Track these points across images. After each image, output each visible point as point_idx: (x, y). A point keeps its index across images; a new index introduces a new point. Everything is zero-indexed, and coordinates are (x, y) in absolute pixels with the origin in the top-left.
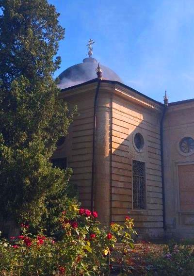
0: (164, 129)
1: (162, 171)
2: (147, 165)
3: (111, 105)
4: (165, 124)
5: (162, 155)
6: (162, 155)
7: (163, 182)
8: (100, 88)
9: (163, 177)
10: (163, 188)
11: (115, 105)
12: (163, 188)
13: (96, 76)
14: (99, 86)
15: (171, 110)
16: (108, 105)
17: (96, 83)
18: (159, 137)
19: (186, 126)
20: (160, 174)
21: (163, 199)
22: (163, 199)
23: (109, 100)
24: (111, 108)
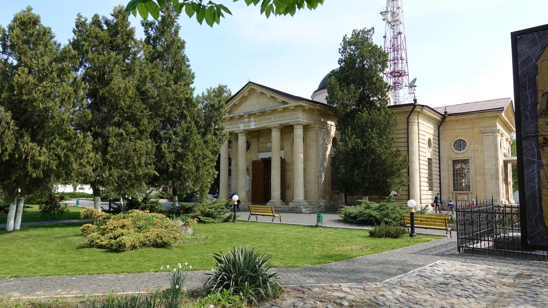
0: (441, 133)
1: (439, 164)
2: (433, 161)
3: (418, 120)
4: (441, 128)
5: (439, 152)
6: (439, 152)
7: (440, 172)
8: (415, 109)
9: (439, 168)
10: (440, 175)
11: (420, 121)
12: (440, 175)
13: (413, 102)
14: (414, 108)
15: (448, 119)
16: (417, 121)
17: (413, 107)
18: (437, 138)
19: (459, 131)
20: (438, 166)
21: (440, 183)
22: (440, 183)
23: (416, 117)
24: (418, 123)
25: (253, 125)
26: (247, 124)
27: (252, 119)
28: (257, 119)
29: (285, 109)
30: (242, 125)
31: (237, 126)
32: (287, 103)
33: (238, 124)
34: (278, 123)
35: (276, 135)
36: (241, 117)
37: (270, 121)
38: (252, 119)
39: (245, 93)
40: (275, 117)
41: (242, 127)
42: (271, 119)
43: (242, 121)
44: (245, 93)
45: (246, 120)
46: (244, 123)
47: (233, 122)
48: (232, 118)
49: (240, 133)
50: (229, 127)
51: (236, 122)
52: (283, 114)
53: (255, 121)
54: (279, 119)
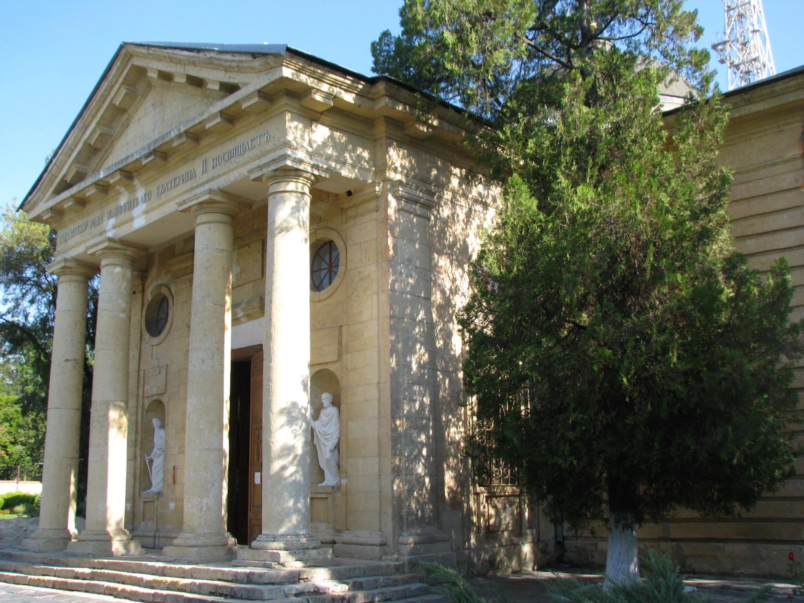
26: (123, 216)
28: (154, 188)
29: (231, 117)
30: (112, 222)
31: (97, 230)
34: (214, 185)
37: (188, 185)
39: (118, 95)
40: (205, 162)
41: (111, 228)
43: (112, 206)
44: (118, 95)
45: (123, 200)
46: (119, 211)
52: (230, 146)
54: (217, 171)
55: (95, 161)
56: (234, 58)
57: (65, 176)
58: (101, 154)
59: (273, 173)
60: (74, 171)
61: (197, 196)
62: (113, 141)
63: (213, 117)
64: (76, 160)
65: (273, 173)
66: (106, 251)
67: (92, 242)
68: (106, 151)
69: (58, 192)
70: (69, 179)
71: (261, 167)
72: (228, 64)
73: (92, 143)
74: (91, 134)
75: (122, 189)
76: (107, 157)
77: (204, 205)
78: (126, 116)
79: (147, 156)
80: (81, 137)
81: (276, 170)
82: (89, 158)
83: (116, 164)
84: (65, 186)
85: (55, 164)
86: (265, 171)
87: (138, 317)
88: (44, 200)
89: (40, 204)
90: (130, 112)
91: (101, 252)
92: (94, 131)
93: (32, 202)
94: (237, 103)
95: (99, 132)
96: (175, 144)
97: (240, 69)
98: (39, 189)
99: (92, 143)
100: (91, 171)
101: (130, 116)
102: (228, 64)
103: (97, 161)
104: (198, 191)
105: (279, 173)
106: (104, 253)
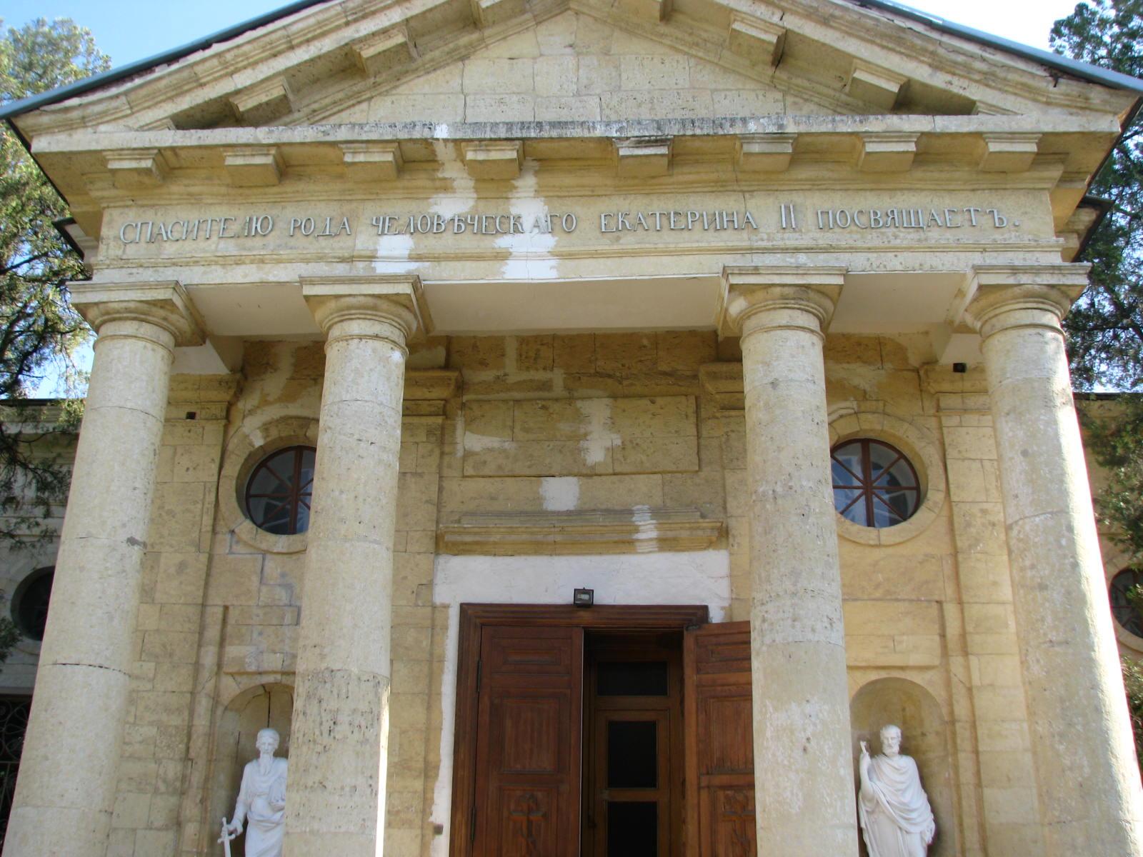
25: (532, 257)
27: (528, 205)
32: (966, 108)
33: (344, 228)
35: (788, 374)
36: (413, 161)
37: (730, 238)
38: (528, 205)
41: (394, 255)
42: (748, 225)
46: (427, 226)
47: (290, 213)
48: (287, 168)
49: (373, 307)
50: (229, 247)
51: (322, 211)
53: (560, 224)
55: (336, 92)
56: (986, 55)
57: (238, 92)
58: (360, 86)
59: (1045, 290)
60: (276, 92)
61: (799, 270)
62: (407, 72)
63: (901, 136)
64: (291, 74)
65: (1045, 290)
66: (384, 305)
67: (322, 269)
68: (375, 85)
69: (183, 122)
70: (244, 105)
71: (1014, 270)
72: (960, 59)
73: (367, 53)
74: (374, 34)
75: (463, 181)
76: (370, 99)
77: (812, 294)
78: (475, 36)
79: (641, 142)
80: (338, 28)
81: (1052, 286)
82: (316, 81)
83: (510, 126)
84: (222, 114)
85: (219, 55)
86: (1025, 279)
87: (207, 471)
88: (131, 122)
89: (103, 128)
90: (487, 32)
91: (370, 301)
92: (385, 32)
93: (75, 115)
94: (979, 135)
95: (400, 39)
96: (756, 148)
97: (987, 79)
98: (126, 93)
99: (367, 53)
100: (306, 111)
101: (483, 40)
102: (960, 59)
103: (340, 95)
104: (821, 260)
105: (1054, 294)
106: (374, 308)
